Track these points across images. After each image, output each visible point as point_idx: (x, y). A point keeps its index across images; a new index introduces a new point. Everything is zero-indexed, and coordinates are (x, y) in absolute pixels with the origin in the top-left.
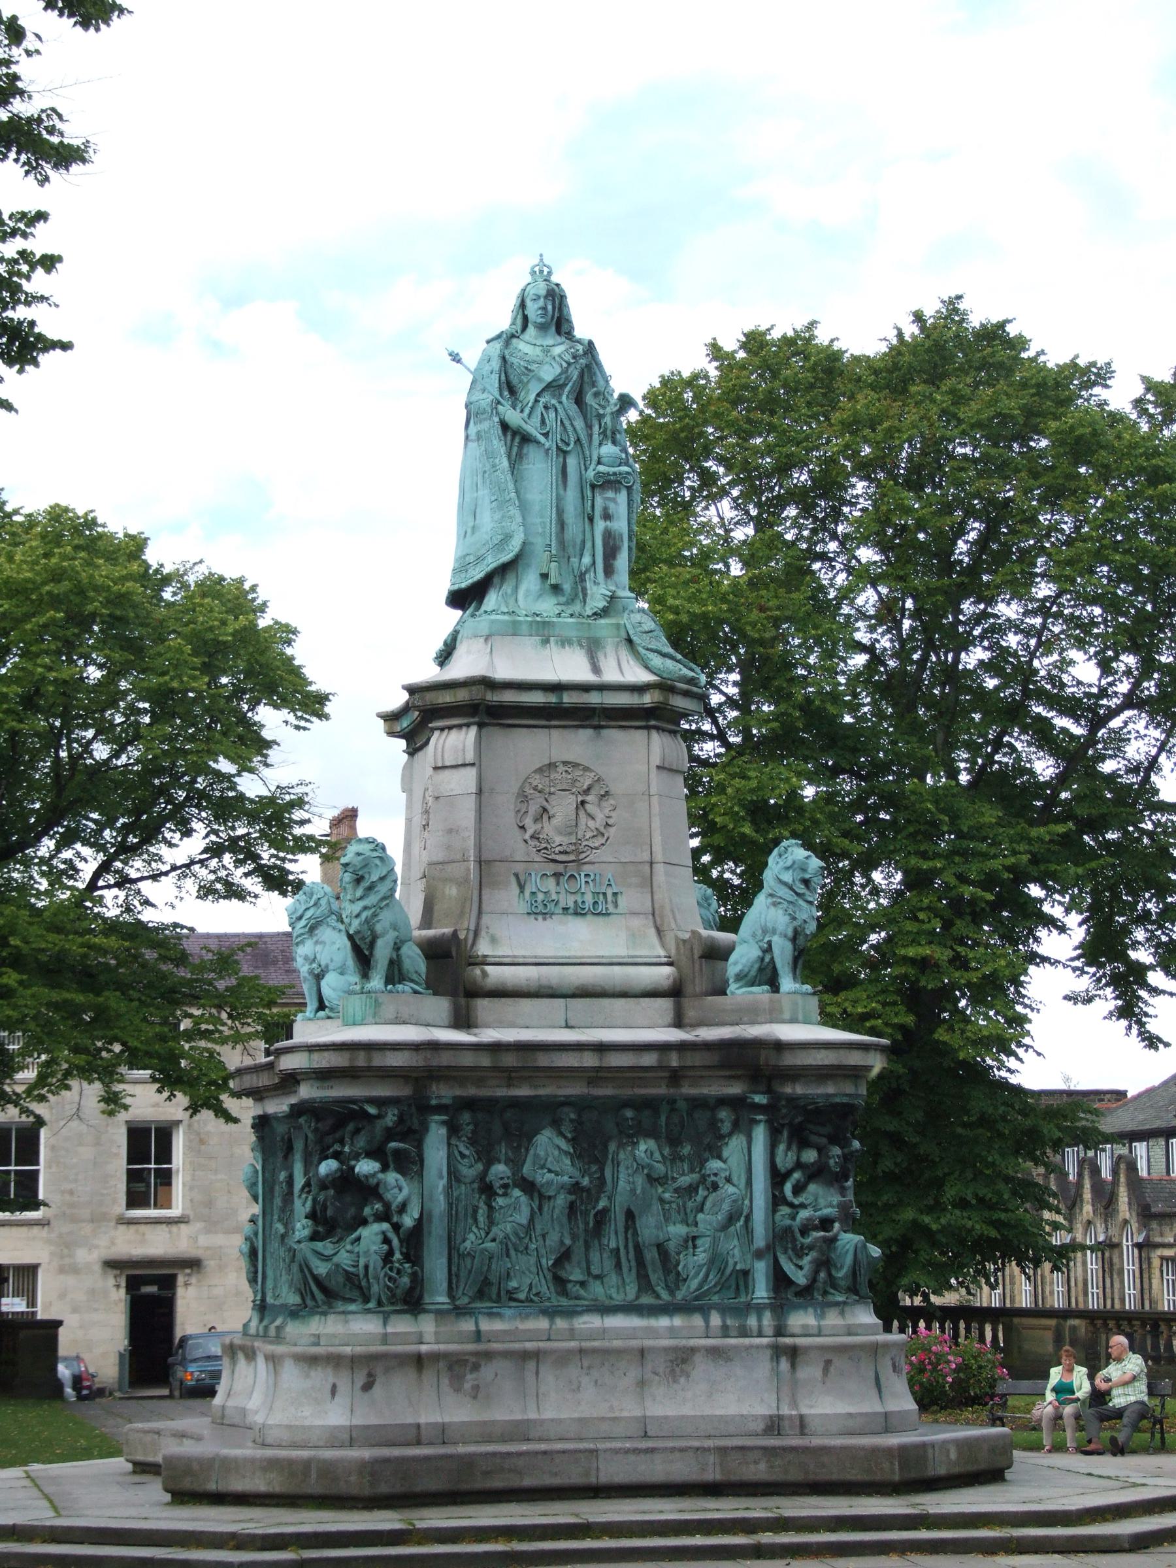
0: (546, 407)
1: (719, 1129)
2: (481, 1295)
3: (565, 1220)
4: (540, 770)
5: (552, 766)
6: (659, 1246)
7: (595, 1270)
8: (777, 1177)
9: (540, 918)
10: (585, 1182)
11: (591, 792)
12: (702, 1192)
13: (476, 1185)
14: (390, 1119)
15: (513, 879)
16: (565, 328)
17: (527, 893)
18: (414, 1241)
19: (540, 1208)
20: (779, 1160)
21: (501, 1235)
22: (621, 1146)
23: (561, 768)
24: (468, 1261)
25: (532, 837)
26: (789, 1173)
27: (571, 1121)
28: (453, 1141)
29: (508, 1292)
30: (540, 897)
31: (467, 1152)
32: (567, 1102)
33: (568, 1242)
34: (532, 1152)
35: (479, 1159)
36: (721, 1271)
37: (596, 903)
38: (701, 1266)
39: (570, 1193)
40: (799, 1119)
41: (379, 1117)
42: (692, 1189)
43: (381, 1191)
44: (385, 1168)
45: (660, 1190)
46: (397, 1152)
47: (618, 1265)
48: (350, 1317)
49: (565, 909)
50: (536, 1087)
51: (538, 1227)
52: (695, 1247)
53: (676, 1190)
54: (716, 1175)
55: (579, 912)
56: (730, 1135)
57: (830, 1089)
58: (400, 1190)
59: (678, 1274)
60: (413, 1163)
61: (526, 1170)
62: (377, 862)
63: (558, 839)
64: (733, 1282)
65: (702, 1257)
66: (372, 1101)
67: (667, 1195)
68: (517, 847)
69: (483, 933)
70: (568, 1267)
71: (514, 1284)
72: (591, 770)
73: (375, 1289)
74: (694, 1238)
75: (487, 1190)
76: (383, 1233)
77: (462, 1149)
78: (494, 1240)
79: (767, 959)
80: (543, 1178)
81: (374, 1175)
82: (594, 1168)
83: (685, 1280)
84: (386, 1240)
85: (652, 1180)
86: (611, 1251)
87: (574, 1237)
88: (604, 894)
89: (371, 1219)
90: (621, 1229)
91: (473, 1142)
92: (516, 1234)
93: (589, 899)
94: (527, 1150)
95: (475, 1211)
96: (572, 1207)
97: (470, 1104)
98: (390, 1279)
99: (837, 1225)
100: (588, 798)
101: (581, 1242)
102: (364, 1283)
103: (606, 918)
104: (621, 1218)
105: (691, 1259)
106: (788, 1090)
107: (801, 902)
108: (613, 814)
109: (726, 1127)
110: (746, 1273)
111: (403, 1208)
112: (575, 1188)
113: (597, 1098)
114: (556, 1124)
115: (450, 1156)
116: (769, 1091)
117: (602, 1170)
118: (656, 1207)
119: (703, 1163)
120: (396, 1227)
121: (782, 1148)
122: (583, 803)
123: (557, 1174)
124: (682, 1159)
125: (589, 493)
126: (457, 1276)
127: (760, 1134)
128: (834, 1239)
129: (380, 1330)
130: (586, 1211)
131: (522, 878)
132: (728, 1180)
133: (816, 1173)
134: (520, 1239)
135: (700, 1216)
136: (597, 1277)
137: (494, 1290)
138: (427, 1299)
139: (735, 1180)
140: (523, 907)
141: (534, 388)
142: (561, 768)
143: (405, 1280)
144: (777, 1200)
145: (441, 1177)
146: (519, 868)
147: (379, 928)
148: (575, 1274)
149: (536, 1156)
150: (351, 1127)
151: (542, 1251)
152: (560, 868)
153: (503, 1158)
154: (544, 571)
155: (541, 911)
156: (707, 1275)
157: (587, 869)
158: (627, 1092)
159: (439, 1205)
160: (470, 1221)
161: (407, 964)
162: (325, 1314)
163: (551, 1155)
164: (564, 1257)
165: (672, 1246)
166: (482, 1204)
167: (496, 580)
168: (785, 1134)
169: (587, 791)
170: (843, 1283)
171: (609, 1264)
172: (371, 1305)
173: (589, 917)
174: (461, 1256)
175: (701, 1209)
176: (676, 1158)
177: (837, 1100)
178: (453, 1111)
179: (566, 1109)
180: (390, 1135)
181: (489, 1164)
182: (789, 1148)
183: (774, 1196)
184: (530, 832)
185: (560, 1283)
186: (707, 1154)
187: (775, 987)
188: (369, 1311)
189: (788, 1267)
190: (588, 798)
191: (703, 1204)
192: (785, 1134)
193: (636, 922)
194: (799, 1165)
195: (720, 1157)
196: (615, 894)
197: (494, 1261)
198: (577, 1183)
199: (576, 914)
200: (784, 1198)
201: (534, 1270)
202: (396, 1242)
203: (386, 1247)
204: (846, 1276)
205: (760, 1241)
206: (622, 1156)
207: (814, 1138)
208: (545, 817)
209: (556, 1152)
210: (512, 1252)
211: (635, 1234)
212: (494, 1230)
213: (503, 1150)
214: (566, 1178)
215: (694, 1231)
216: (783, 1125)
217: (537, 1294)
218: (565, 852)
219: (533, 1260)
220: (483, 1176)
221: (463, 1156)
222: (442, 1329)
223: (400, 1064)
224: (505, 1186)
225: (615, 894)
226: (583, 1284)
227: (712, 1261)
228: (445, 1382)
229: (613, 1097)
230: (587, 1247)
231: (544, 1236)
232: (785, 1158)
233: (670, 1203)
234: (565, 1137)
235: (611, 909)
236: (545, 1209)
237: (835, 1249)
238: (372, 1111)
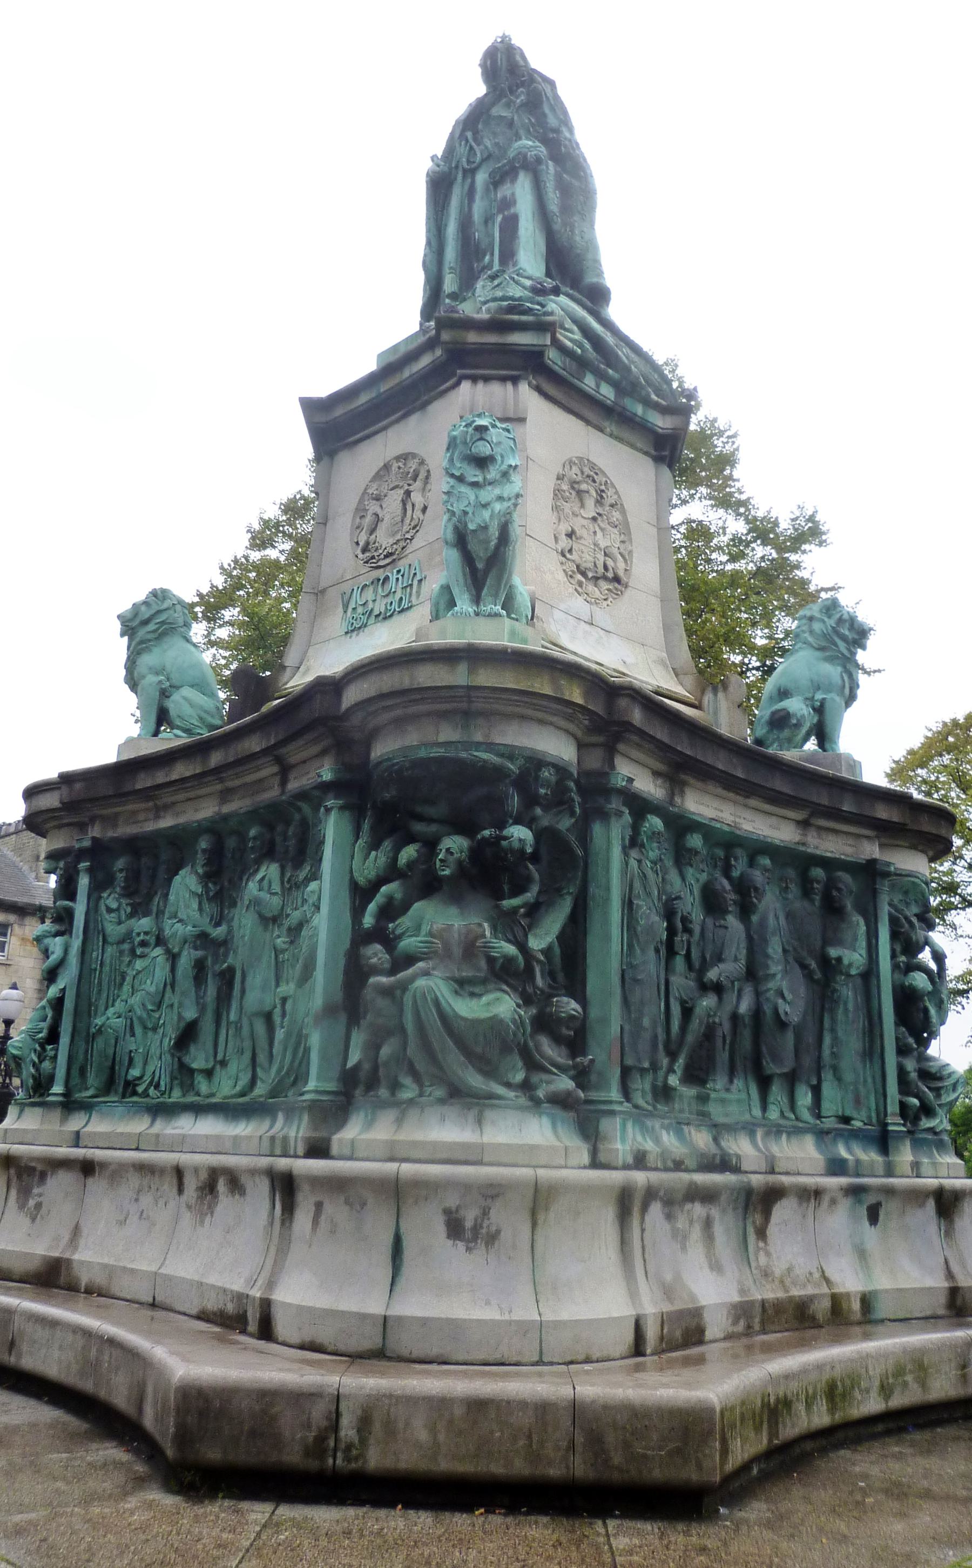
2: (108, 1087)
5: (386, 467)
29: (128, 1083)
39: (196, 949)
50: (177, 815)
71: (135, 1072)
87: (202, 1009)
91: (129, 892)
112: (202, 939)
133: (428, 885)
161: (173, 712)
164: (187, 1036)
177: (422, 753)
194: (392, 873)
198: (203, 936)
207: (419, 827)
210: (138, 1030)
221: (110, 910)
222: (45, 1127)
228: (13, 1193)
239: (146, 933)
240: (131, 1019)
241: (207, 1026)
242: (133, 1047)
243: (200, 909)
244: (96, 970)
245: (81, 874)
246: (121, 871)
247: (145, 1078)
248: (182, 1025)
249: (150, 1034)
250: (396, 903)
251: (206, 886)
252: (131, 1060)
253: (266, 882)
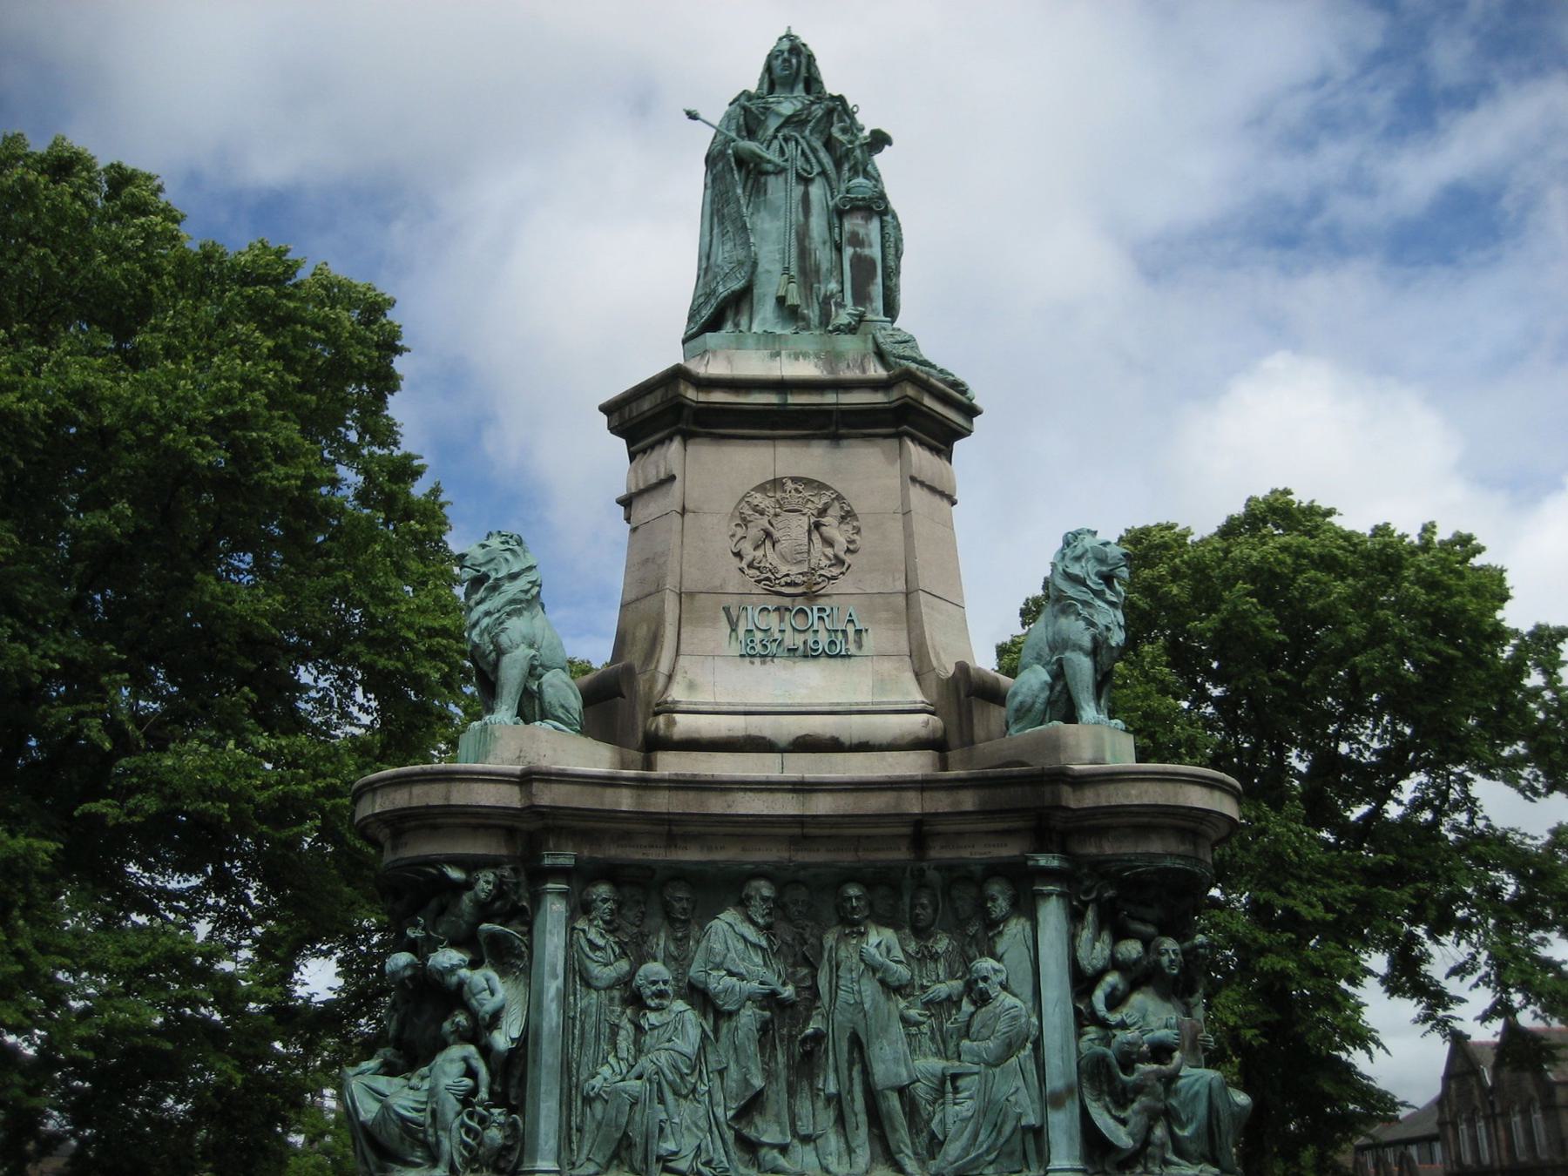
0: (786, 140)
1: (987, 912)
3: (753, 1048)
4: (761, 488)
5: (777, 483)
6: (901, 1091)
7: (805, 1128)
8: (1082, 982)
9: (757, 661)
10: (788, 991)
11: (828, 506)
12: (967, 1007)
13: (616, 994)
14: (485, 883)
15: (723, 614)
16: (814, 87)
17: (741, 631)
18: (510, 1075)
19: (716, 1030)
20: (1082, 953)
21: (651, 1068)
22: (844, 937)
23: (790, 485)
24: (598, 1106)
25: (750, 566)
26: (1100, 975)
27: (765, 899)
28: (581, 924)
29: (659, 1158)
30: (759, 636)
31: (601, 942)
32: (758, 873)
33: (758, 1082)
34: (704, 944)
35: (624, 954)
36: (997, 1127)
37: (832, 643)
38: (967, 1120)
39: (763, 1008)
40: (1109, 893)
41: (468, 885)
42: (952, 1002)
43: (466, 995)
44: (474, 965)
45: (902, 1004)
46: (493, 938)
47: (841, 1121)
49: (792, 651)
50: (710, 849)
51: (711, 1058)
52: (956, 1090)
53: (927, 1004)
54: (985, 979)
55: (810, 654)
56: (1005, 920)
57: (1156, 847)
58: (492, 993)
59: (933, 1136)
60: (520, 956)
61: (695, 971)
62: (508, 555)
63: (784, 569)
64: (1016, 1143)
65: (966, 1108)
66: (456, 862)
67: (913, 1013)
68: (730, 575)
69: (678, 678)
70: (758, 1120)
71: (670, 1146)
72: (828, 488)
73: (446, 1145)
74: (955, 1077)
75: (636, 1000)
76: (465, 1059)
77: (593, 935)
78: (639, 1077)
79: (1058, 688)
80: (718, 982)
81: (453, 969)
82: (804, 971)
83: (942, 1144)
84: (470, 1073)
85: (893, 989)
86: (829, 1099)
87: (769, 1075)
88: (844, 632)
89: (451, 1039)
90: (844, 1065)
91: (611, 928)
92: (676, 1068)
93: (824, 638)
94: (698, 942)
95: (615, 1029)
96: (765, 1028)
97: (612, 873)
98: (469, 1130)
99: (1177, 1055)
100: (824, 520)
101: (783, 1084)
103: (847, 661)
104: (844, 1046)
105: (952, 1110)
106: (1091, 849)
107: (1098, 602)
108: (856, 537)
109: (1001, 905)
110: (1038, 1133)
111: (496, 1018)
113: (804, 866)
114: (743, 903)
115: (569, 945)
116: (1064, 850)
117: (814, 977)
118: (898, 1029)
119: (967, 961)
120: (486, 1051)
121: (1086, 934)
122: (818, 526)
123: (742, 977)
124: (935, 957)
125: (836, 221)
126: (579, 1130)
127: (1052, 914)
128: (1174, 1077)
130: (794, 1036)
131: (734, 613)
132: (1005, 987)
133: (1141, 976)
134: (682, 1076)
135: (966, 1043)
136: (806, 1139)
137: (638, 1155)
139: (1013, 985)
140: (736, 649)
141: (773, 124)
142: (790, 485)
143: (495, 1135)
144: (1084, 1018)
145: (555, 977)
146: (731, 601)
147: (504, 639)
148: (768, 1131)
149: (710, 950)
151: (719, 1097)
152: (787, 602)
153: (661, 954)
154: (781, 293)
155: (760, 652)
156: (976, 1135)
157: (822, 602)
158: (847, 858)
159: (552, 1017)
160: (605, 1046)
161: (550, 695)
163: (733, 948)
164: (752, 1106)
165: (921, 1090)
166: (625, 1022)
167: (730, 314)
168: (1090, 915)
169: (823, 512)
170: (1192, 1147)
171: (827, 1118)
173: (823, 660)
174: (588, 1101)
175: (966, 1033)
176: (926, 957)
177: (1168, 863)
178: (580, 877)
179: (755, 884)
180: (485, 911)
181: (641, 960)
182: (1096, 937)
183: (1077, 1012)
184: (747, 559)
185: (750, 1147)
186: (973, 951)
187: (1071, 716)
189: (1103, 1120)
190: (824, 520)
191: (968, 1025)
192: (1090, 915)
193: (887, 666)
194: (1115, 964)
195: (993, 955)
196: (858, 632)
197: (638, 1108)
198: (774, 993)
199: (806, 656)
200: (1093, 1012)
201: (703, 1123)
203: (468, 1082)
204: (1196, 1136)
205: (1056, 1079)
206: (843, 954)
208: (768, 544)
209: (741, 946)
210: (669, 1097)
211: (866, 1073)
212: (643, 1060)
213: (661, 942)
214: (755, 984)
215: (954, 1066)
216: (1086, 905)
217: (708, 1163)
218: (793, 584)
219: (702, 1110)
220: (625, 981)
221: (594, 947)
223: (491, 802)
224: (661, 994)
225: (858, 632)
226: (784, 1149)
227: (983, 1112)
229: (825, 865)
230: (792, 1092)
231: (721, 1072)
232: (1095, 952)
233: (918, 1024)
234: (755, 924)
235: (853, 650)
236: (724, 1030)
237: (1177, 1092)
238: (455, 874)
239: (665, 982)
240: (659, 1084)
241: (778, 1096)
242: (663, 1116)
243: (765, 964)
244: (574, 1018)
245: (549, 899)
246: (605, 901)
247: (683, 1153)
248: (749, 1095)
249: (682, 1101)
250: (1118, 993)
251: (768, 939)
252: (661, 1130)
253: (883, 946)
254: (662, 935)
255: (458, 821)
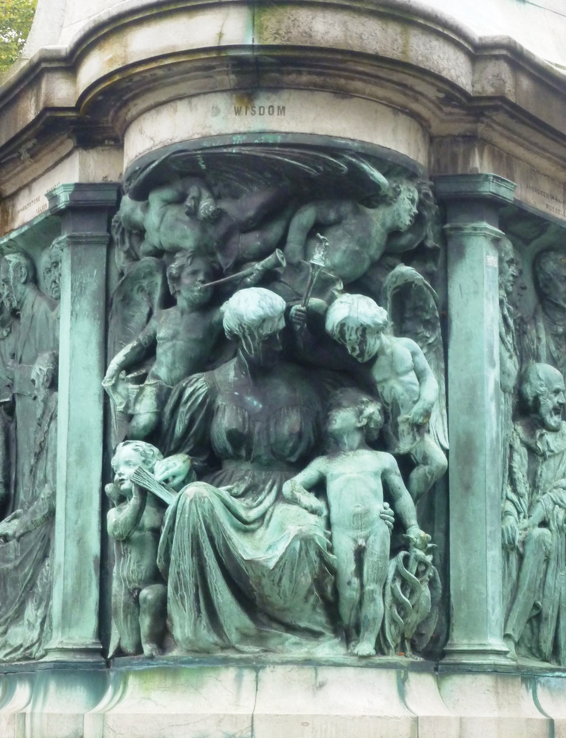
18: (436, 500)
43: (378, 374)
48: (326, 674)
60: (427, 324)
73: (378, 608)
98: (405, 583)
102: (350, 593)
129: (394, 709)
138: (460, 641)
150: (306, 216)
162: (256, 666)
172: (366, 647)
188: (365, 662)
202: (407, 502)
254: (541, 325)
255: (380, 92)
